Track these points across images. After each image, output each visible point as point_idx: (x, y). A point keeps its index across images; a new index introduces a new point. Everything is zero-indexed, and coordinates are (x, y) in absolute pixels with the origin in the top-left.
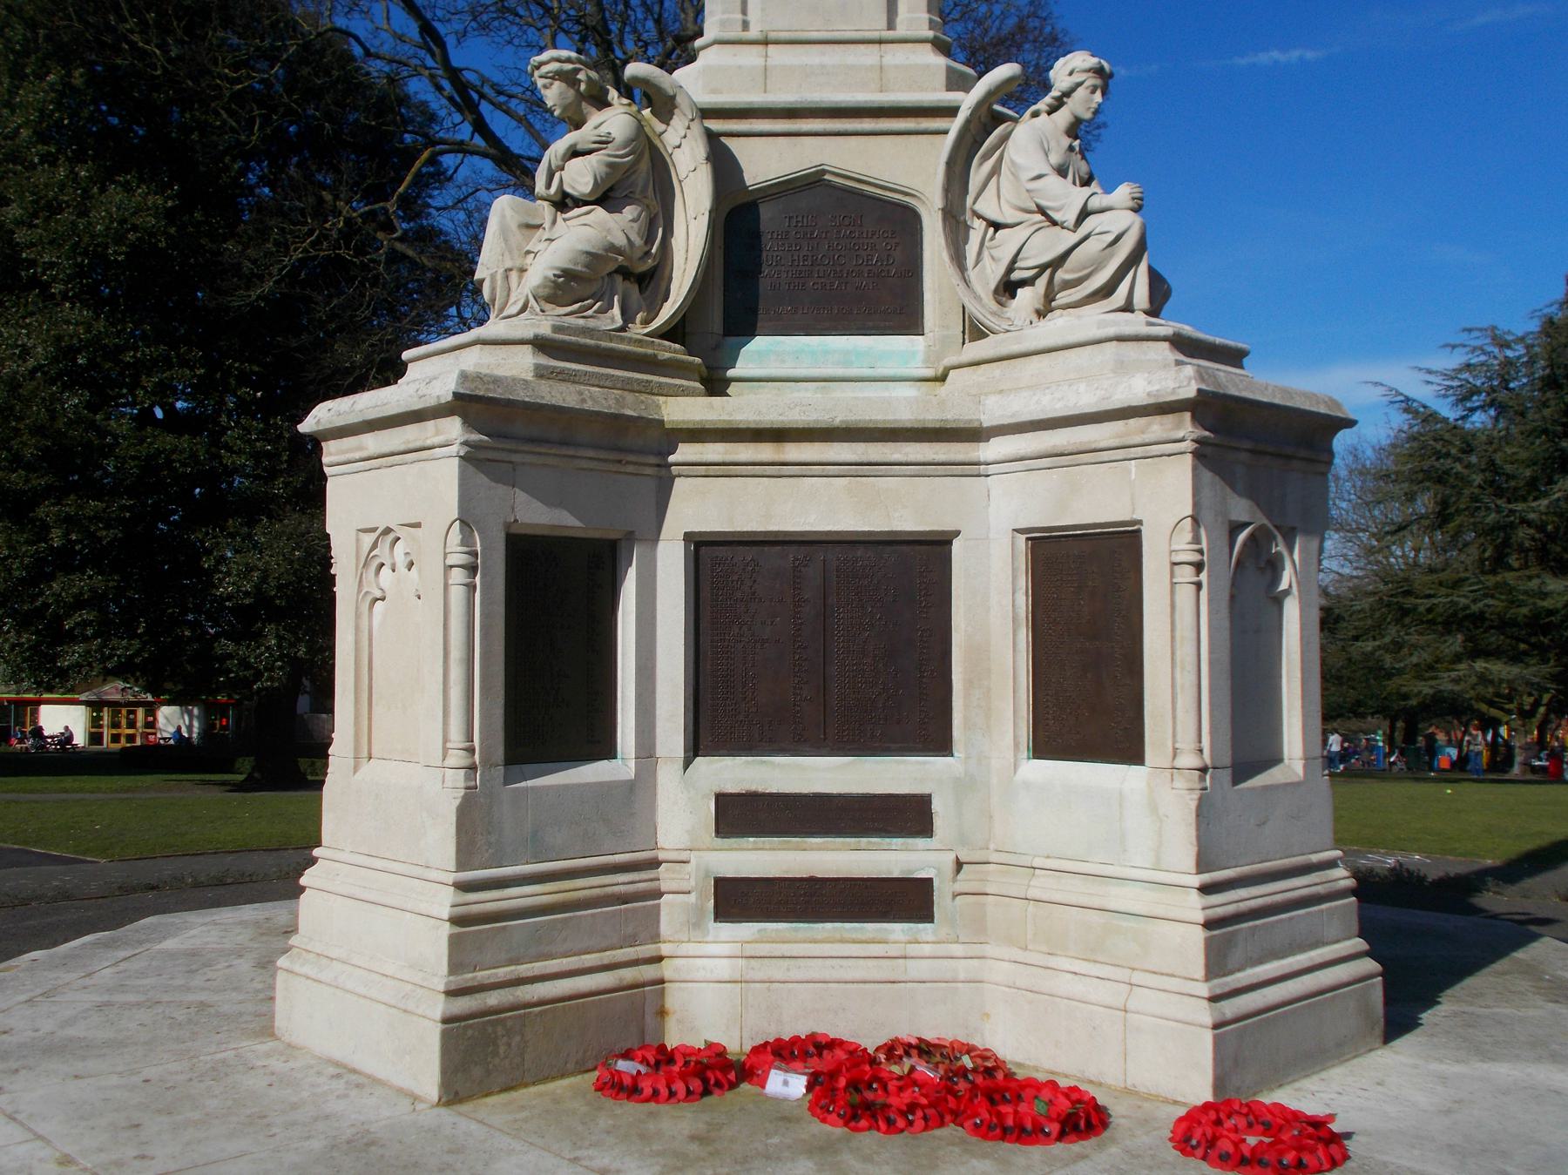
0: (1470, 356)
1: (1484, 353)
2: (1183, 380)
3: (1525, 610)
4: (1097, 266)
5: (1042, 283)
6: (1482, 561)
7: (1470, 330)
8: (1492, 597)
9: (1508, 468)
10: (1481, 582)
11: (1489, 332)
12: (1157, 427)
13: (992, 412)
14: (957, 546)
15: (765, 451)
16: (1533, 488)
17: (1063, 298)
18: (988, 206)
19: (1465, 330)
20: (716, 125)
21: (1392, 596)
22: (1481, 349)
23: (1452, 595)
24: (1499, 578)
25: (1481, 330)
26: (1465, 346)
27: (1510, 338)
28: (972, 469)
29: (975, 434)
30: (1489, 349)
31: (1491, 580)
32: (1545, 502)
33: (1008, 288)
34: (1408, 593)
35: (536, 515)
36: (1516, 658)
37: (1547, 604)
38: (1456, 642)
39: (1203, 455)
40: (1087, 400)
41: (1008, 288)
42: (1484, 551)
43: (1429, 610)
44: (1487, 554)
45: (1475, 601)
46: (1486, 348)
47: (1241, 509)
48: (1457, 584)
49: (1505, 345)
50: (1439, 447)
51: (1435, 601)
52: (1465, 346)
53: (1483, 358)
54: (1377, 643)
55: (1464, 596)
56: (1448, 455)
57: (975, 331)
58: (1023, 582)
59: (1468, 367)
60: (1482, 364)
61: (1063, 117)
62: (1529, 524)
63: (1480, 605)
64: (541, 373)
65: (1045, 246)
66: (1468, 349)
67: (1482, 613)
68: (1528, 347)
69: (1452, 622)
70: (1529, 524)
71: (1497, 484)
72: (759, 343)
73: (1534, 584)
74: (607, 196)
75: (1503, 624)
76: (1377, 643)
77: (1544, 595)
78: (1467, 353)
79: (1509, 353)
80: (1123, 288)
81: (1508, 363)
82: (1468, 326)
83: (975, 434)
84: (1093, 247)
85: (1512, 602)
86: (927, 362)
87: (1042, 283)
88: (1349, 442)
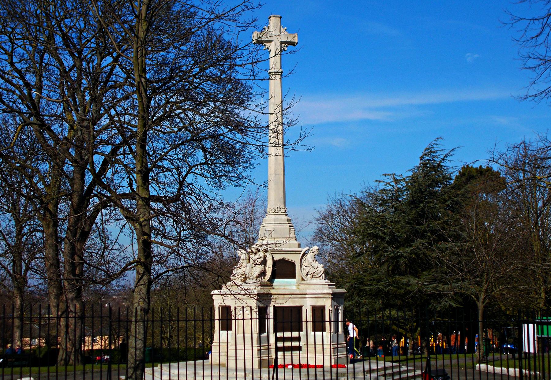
0: (385, 187)
1: (390, 185)
2: (330, 291)
3: (402, 291)
4: (319, 274)
5: (312, 274)
6: (388, 271)
7: (385, 175)
8: (392, 285)
9: (398, 234)
10: (387, 280)
11: (392, 177)
12: (327, 296)
13: (308, 292)
14: (303, 307)
15: (282, 296)
16: (408, 242)
17: (314, 276)
18: (304, 264)
19: (383, 175)
20: (272, 252)
21: (355, 284)
22: (389, 183)
23: (378, 285)
24: (394, 279)
25: (390, 175)
26: (384, 182)
27: (399, 178)
28: (305, 298)
29: (306, 294)
30: (392, 184)
31: (390, 280)
32: (409, 250)
33: (307, 274)
34: (362, 283)
35: (261, 305)
36: (399, 309)
37: (409, 288)
38: (379, 304)
39: (332, 299)
40: (319, 292)
41: (307, 274)
42: (389, 267)
43: (370, 290)
44: (390, 268)
45: (386, 287)
46: (391, 183)
47: (335, 304)
48: (379, 281)
49: (397, 182)
50: (373, 224)
51: (371, 287)
52: (384, 182)
53: (390, 187)
54: (350, 303)
55: (382, 285)
56: (377, 228)
57: (303, 279)
58: (311, 312)
59: (383, 191)
60: (390, 190)
61: (314, 254)
62: (405, 257)
63: (387, 289)
64: (261, 289)
65: (312, 271)
66: (385, 183)
67: (388, 291)
68: (407, 183)
69: (376, 295)
70: (405, 257)
71: (394, 240)
72: (276, 280)
73: (405, 280)
74: (261, 264)
75: (396, 296)
76: (350, 303)
77: (409, 285)
78: (384, 185)
79: (399, 186)
80: (322, 276)
81: (399, 190)
82: (384, 173)
83: (306, 294)
84: (318, 272)
85: (398, 288)
86: (297, 283)
87: (312, 274)
88: (338, 197)
